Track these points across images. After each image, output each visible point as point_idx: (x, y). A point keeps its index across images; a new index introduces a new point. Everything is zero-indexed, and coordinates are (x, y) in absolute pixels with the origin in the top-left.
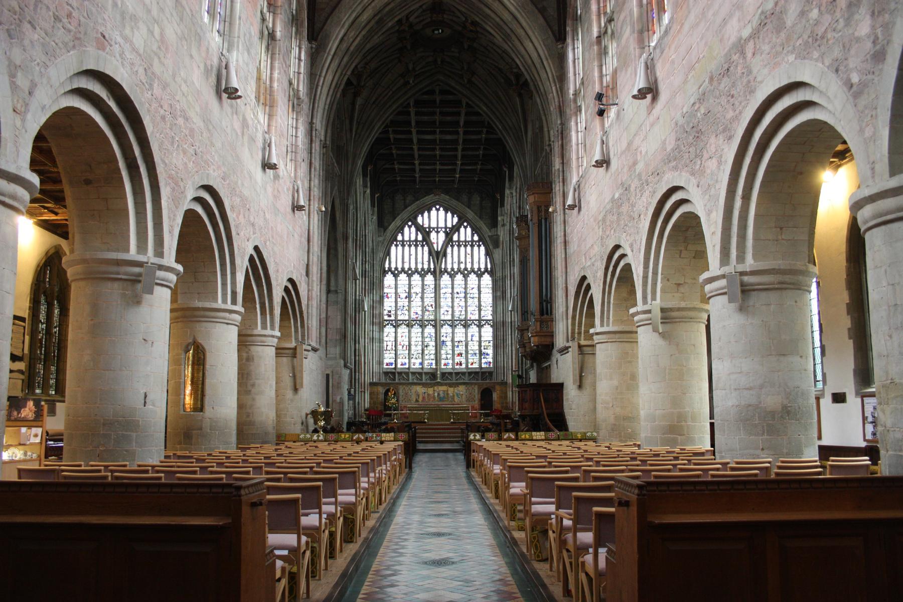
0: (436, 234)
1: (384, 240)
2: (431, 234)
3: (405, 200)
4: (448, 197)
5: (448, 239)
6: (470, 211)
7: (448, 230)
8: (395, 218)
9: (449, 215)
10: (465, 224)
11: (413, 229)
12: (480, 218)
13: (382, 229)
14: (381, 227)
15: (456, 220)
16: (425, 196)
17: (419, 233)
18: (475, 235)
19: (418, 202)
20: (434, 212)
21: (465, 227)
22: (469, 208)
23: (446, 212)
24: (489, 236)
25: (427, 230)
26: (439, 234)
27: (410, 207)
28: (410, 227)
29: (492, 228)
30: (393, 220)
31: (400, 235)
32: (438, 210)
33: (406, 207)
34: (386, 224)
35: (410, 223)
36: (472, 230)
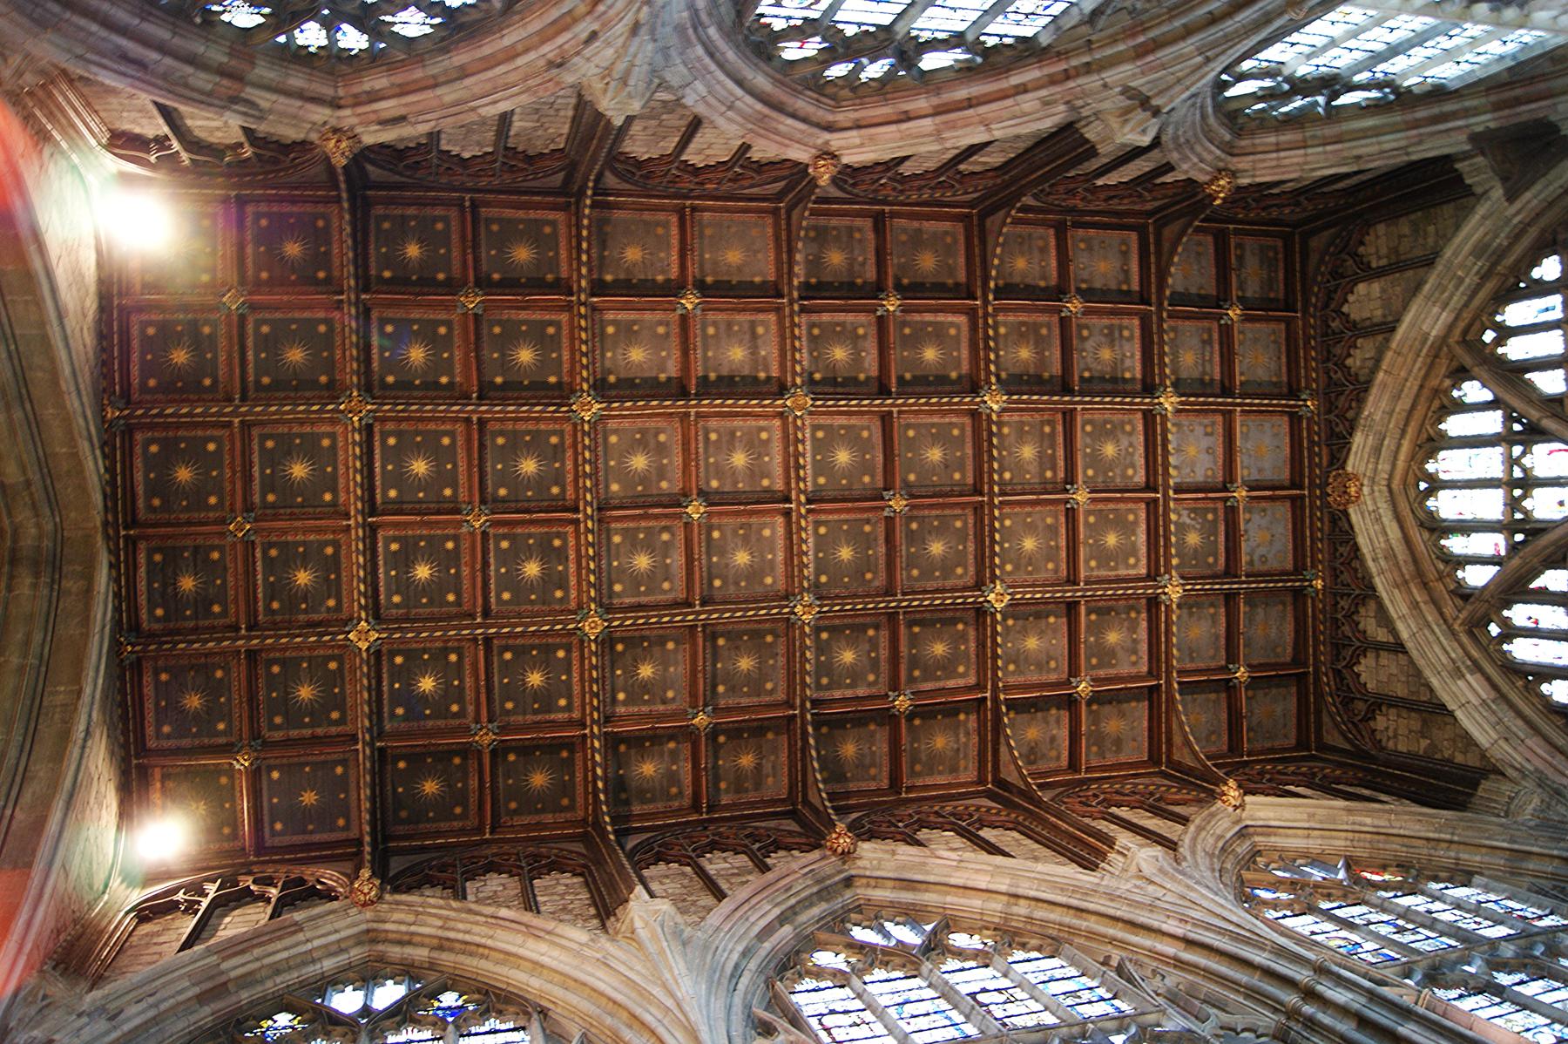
0: (1537, 492)
1: (1542, 782)
2: (1539, 514)
3: (1379, 647)
4: (1358, 439)
5: (1549, 424)
6: (1408, 319)
7: (1517, 427)
8: (1443, 706)
9: (1455, 425)
10: (1489, 336)
11: (1520, 614)
12: (1429, 262)
13: (1485, 784)
14: (1475, 786)
15: (1473, 391)
16: (1356, 548)
17: (1535, 584)
18: (1536, 273)
19: (1379, 582)
20: (1447, 505)
21: (1505, 333)
22: (1393, 330)
23: (1437, 443)
24: (1511, 197)
25: (1519, 537)
26: (1540, 472)
27: (1400, 626)
28: (1511, 632)
29: (1468, 191)
30: (1451, 714)
31: (1545, 688)
32: (1436, 485)
33: (1398, 648)
34: (1472, 760)
35: (1494, 629)
36: (1512, 294)
